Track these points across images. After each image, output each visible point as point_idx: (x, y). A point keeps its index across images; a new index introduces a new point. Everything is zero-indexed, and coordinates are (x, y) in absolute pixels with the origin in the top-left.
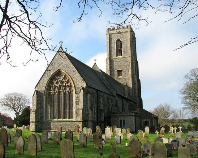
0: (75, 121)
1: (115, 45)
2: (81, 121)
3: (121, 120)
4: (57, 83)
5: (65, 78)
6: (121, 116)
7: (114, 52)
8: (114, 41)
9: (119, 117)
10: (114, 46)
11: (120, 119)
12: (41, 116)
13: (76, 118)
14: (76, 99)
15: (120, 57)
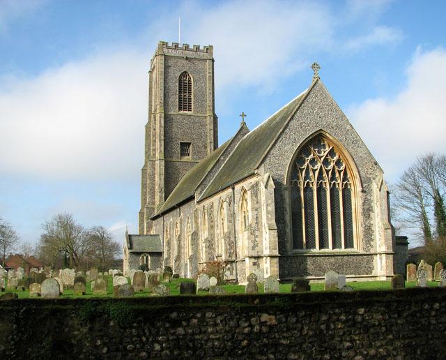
0: (362, 252)
1: (177, 84)
2: (391, 254)
4: (313, 162)
5: (332, 153)
7: (174, 99)
8: (175, 74)
10: (174, 86)
15: (187, 112)
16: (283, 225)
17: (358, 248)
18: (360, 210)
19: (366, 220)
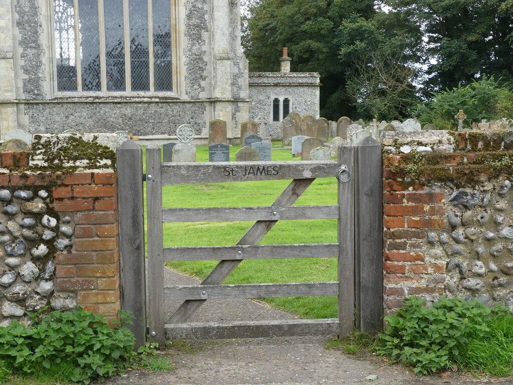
0: (185, 97)
3: (276, 101)
6: (276, 85)
9: (268, 90)
11: (273, 98)
12: (26, 77)
13: (189, 90)
14: (189, 17)
16: (34, 51)
17: (181, 88)
18: (182, 27)
19: (193, 45)
